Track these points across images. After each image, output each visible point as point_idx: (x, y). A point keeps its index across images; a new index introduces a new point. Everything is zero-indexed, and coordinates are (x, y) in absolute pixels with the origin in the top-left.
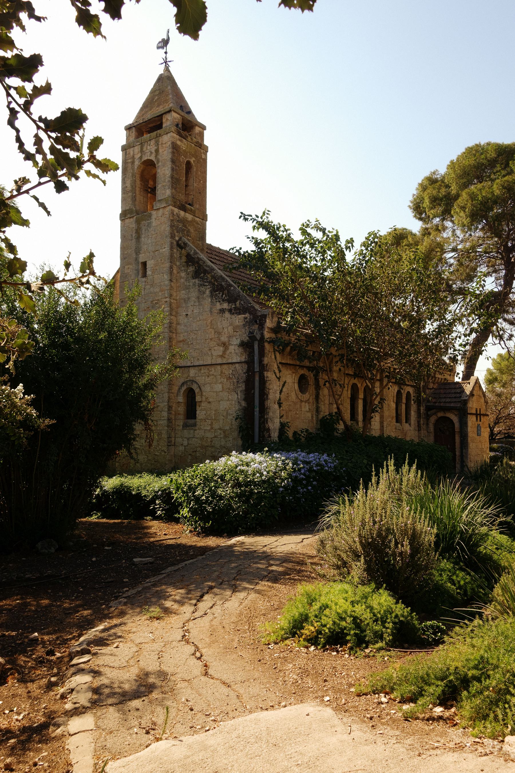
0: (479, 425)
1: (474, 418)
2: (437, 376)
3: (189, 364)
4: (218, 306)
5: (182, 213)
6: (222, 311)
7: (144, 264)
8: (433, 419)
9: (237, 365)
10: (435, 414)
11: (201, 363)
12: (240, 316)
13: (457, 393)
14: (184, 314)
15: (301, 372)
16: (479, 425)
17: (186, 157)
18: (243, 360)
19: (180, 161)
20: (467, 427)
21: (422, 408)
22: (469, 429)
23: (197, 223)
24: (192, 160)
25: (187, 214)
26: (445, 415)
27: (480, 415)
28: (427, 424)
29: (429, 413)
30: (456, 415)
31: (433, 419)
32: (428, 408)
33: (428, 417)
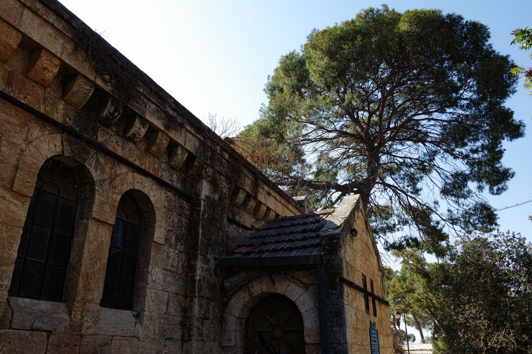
0: (372, 325)
1: (360, 301)
2: (261, 197)
8: (238, 304)
10: (244, 286)
13: (311, 230)
16: (372, 325)
20: (342, 325)
21: (199, 264)
22: (350, 332)
26: (273, 290)
27: (375, 298)
28: (222, 321)
29: (227, 284)
30: (306, 287)
31: (238, 304)
32: (226, 268)
33: (222, 297)
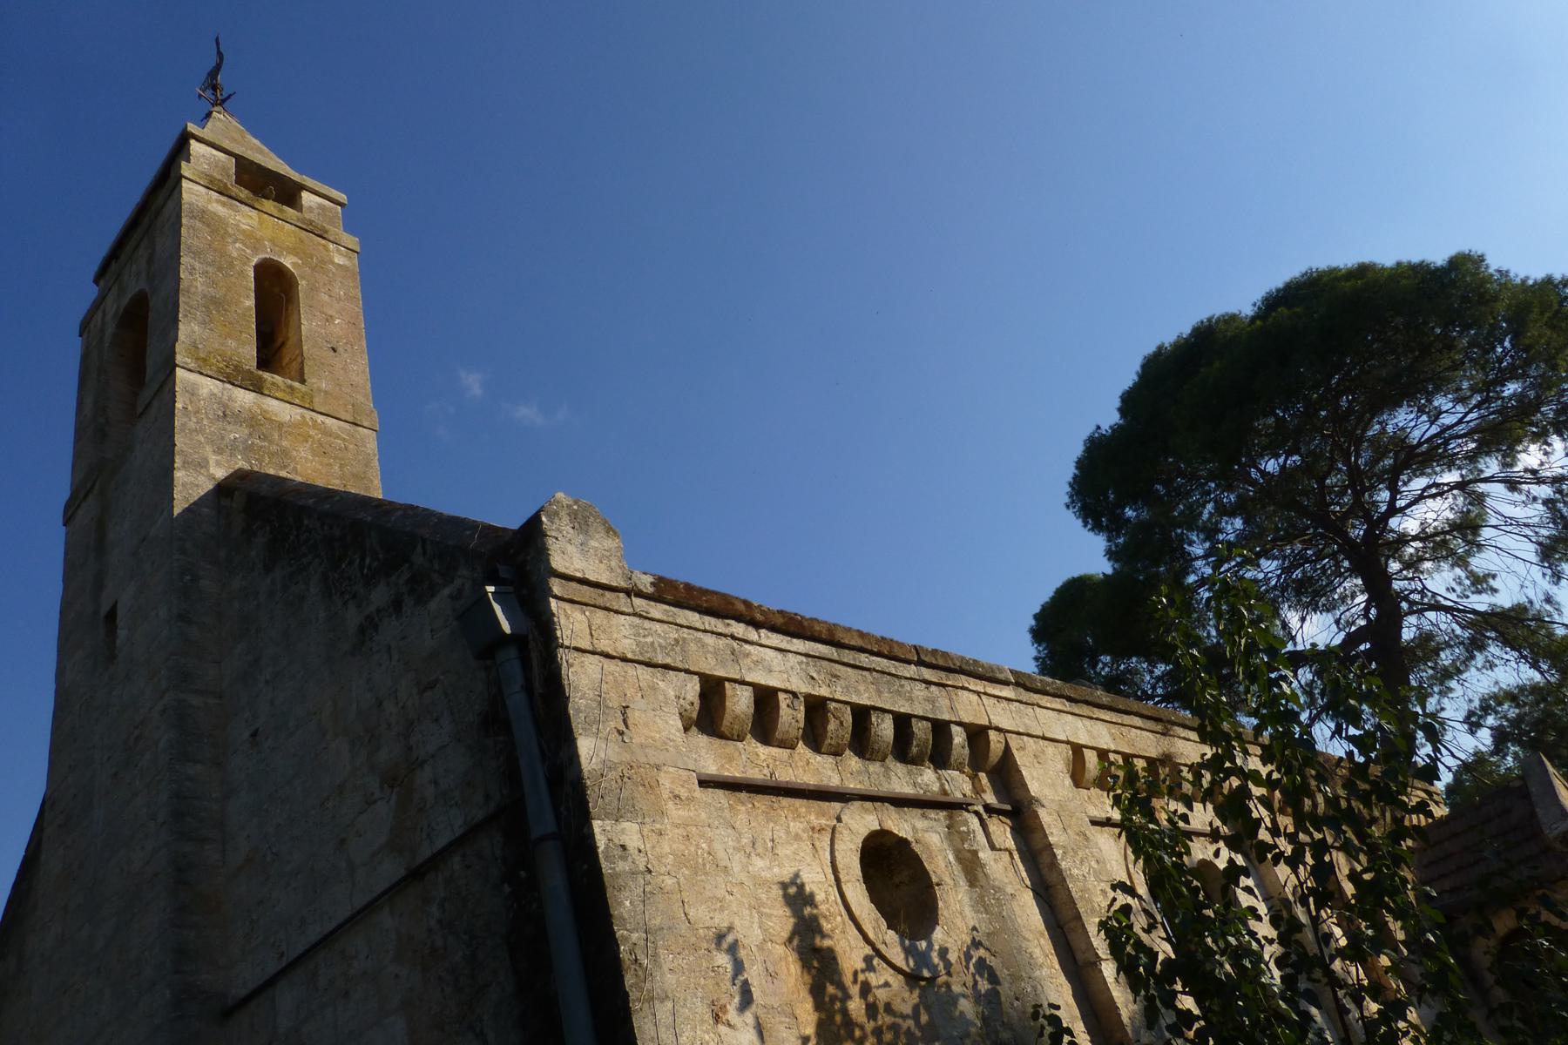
3: (272, 967)
4: (353, 618)
5: (244, 398)
6: (369, 627)
7: (111, 616)
9: (456, 862)
11: (315, 933)
12: (433, 605)
14: (247, 734)
15: (861, 822)
17: (255, 250)
18: (479, 815)
19: (223, 254)
23: (327, 432)
24: (288, 262)
25: (272, 405)
